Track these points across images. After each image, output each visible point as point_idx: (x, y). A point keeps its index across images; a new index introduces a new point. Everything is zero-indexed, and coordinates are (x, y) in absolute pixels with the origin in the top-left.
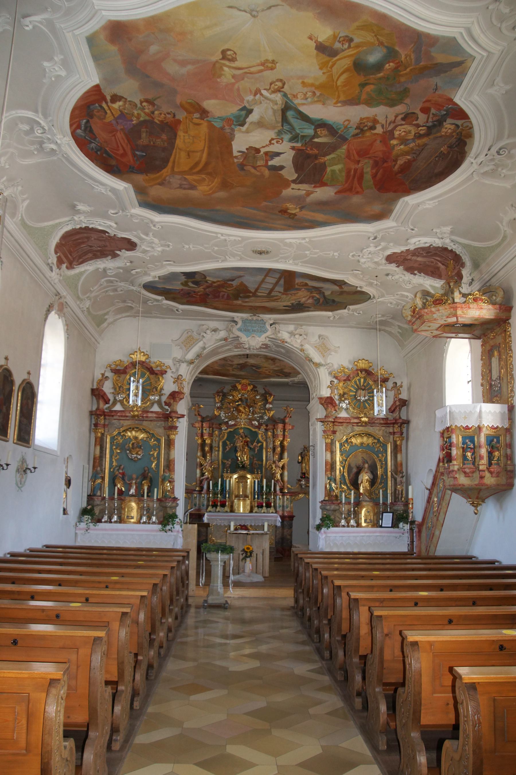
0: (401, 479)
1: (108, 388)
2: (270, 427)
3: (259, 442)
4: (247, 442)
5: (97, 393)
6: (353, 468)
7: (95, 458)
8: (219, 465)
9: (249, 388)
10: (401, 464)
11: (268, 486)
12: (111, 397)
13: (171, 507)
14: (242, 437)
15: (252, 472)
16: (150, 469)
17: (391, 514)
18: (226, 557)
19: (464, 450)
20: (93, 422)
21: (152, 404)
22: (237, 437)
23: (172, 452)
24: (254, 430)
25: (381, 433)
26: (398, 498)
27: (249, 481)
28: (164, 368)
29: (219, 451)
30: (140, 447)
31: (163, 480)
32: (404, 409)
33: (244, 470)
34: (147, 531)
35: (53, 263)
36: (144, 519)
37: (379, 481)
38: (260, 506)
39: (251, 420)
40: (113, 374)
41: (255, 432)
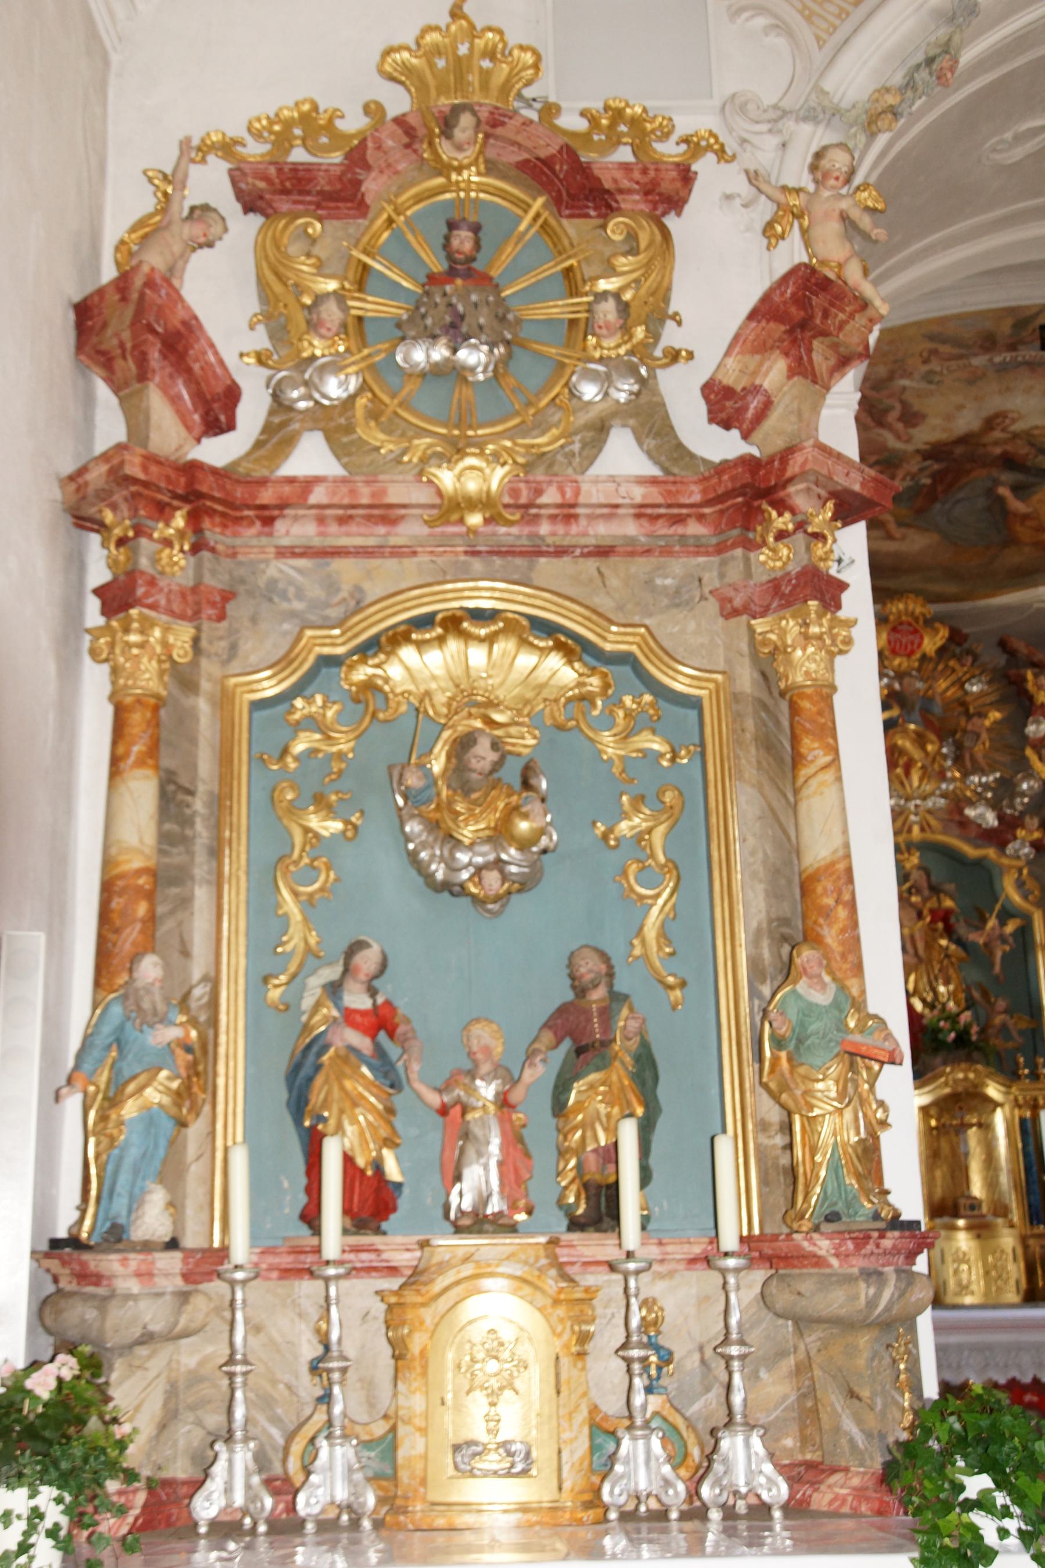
1: (220, 294)
4: (945, 916)
5: (119, 328)
9: (930, 644)
15: (1010, 1075)
20: (98, 572)
21: (600, 430)
24: (970, 851)
27: (999, 1120)
33: (970, 1059)
36: (643, 1467)
41: (979, 863)
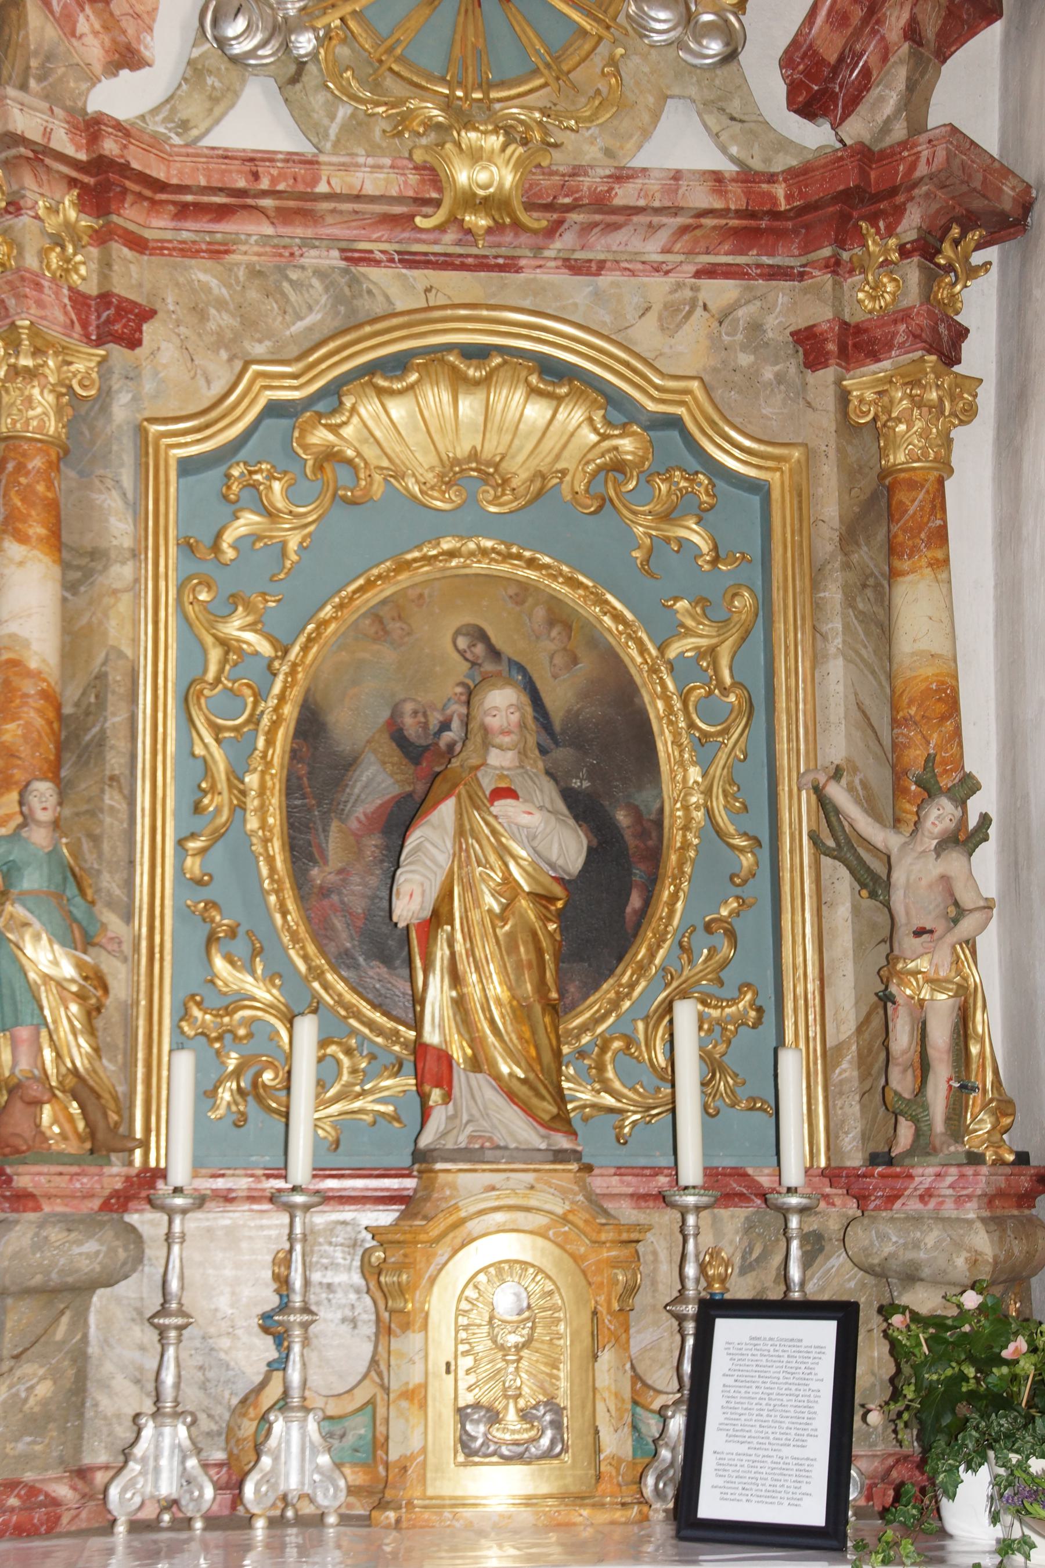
0: (953, 862)
6: (349, 764)
17: (826, 1331)
25: (689, 348)
26: (915, 1107)
37: (676, 905)
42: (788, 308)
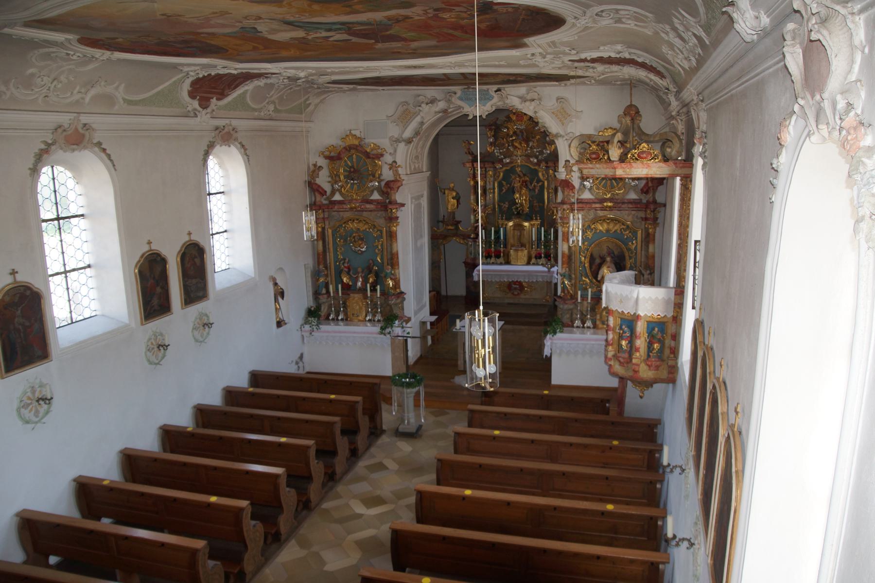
1: (323, 180)
2: (550, 164)
3: (539, 181)
4: (526, 182)
7: (318, 254)
8: (494, 208)
10: (653, 257)
11: (547, 233)
12: (327, 188)
13: (396, 304)
14: (519, 176)
15: (529, 218)
16: (375, 262)
18: (415, 390)
19: (621, 337)
22: (513, 177)
23: (394, 245)
25: (630, 218)
28: (380, 151)
29: (494, 192)
30: (362, 239)
31: (386, 277)
32: (661, 188)
34: (368, 333)
35: (195, 109)
38: (538, 256)
39: (528, 156)
40: (327, 161)
42: (642, 214)
